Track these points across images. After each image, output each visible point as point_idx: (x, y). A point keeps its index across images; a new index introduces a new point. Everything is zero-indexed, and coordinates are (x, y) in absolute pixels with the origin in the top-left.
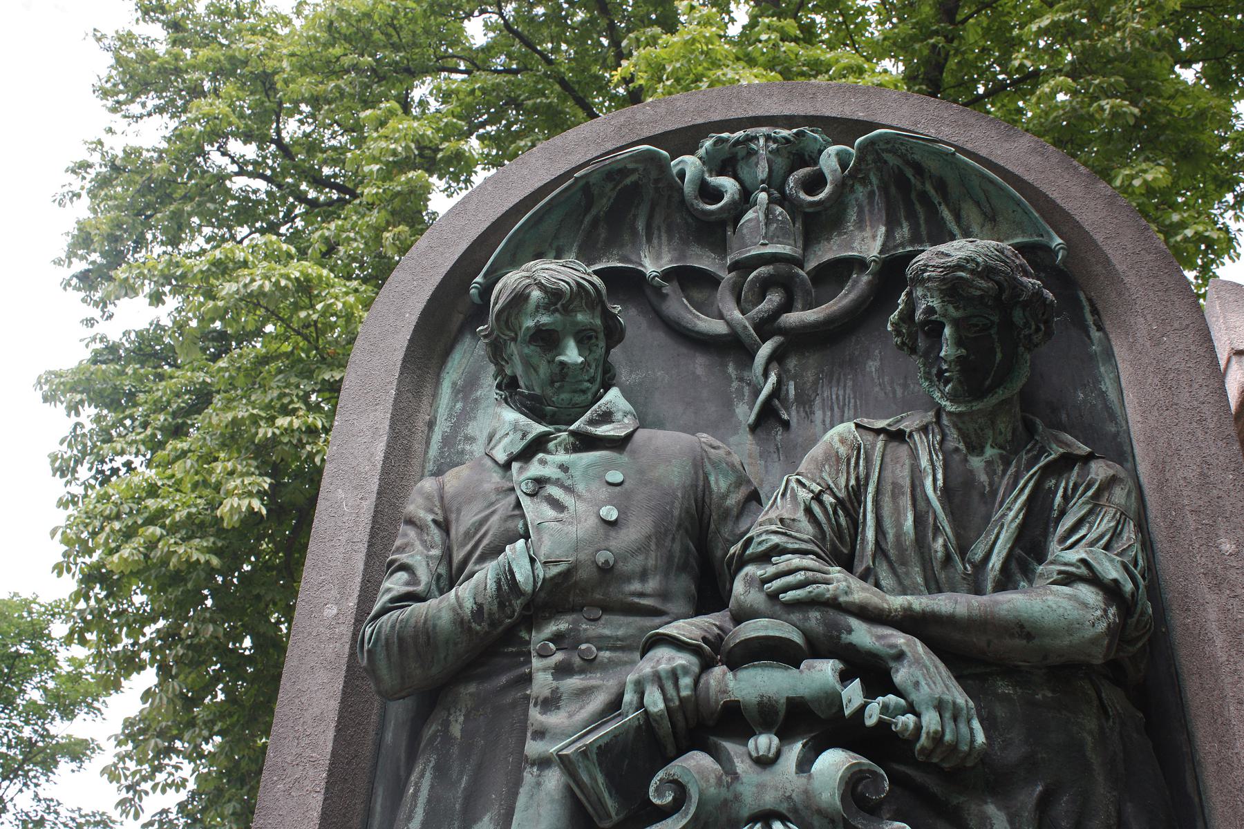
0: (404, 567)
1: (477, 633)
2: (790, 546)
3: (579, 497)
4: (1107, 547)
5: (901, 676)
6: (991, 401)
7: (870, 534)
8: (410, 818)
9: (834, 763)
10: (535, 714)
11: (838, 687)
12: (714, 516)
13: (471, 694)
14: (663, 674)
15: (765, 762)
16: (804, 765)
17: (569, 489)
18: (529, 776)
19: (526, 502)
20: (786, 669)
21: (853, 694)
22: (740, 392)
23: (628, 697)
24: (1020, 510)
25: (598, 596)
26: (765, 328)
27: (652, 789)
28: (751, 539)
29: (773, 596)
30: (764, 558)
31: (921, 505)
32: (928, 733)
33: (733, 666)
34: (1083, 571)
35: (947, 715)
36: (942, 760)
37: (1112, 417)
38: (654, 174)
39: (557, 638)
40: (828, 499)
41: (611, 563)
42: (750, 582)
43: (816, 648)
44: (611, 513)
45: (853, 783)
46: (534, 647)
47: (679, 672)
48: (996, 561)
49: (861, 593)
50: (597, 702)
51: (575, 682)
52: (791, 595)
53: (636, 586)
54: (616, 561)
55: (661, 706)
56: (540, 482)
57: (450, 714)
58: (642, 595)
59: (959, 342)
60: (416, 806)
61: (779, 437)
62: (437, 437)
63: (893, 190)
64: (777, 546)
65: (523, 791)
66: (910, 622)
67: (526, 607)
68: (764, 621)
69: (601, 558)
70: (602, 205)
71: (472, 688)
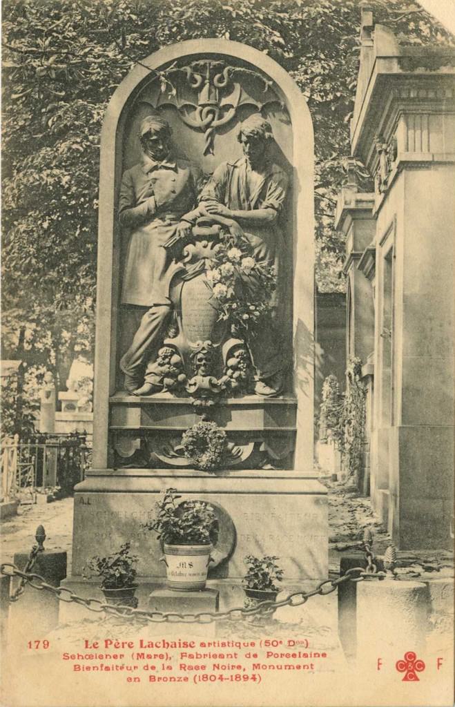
34: (270, 206)
40: (220, 185)
43: (215, 222)
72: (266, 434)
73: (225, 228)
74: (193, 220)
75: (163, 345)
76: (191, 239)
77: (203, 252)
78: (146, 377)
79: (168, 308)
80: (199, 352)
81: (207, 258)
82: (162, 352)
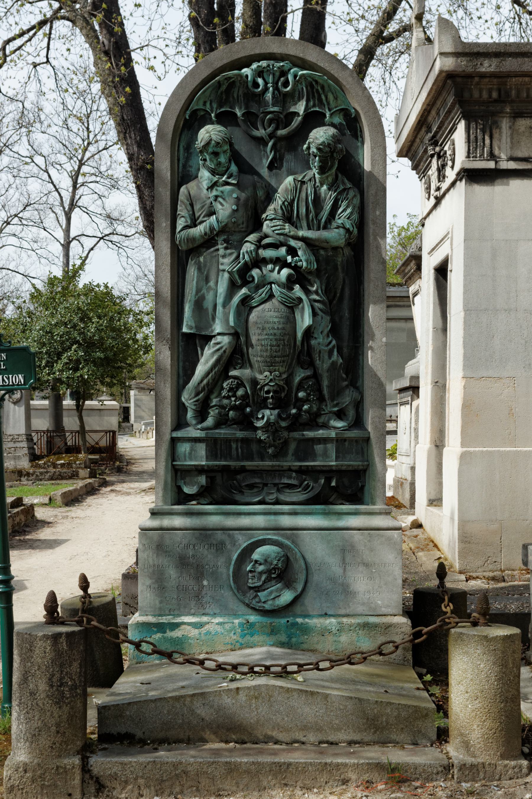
3: (227, 202)
4: (348, 218)
6: (327, 174)
9: (285, 272)
10: (221, 260)
16: (279, 272)
17: (224, 199)
18: (221, 273)
19: (214, 203)
22: (264, 155)
23: (241, 256)
26: (271, 136)
38: (239, 79)
40: (286, 203)
42: (268, 226)
43: (282, 244)
44: (235, 207)
45: (289, 277)
46: (219, 242)
51: (229, 251)
52: (277, 232)
56: (216, 197)
59: (320, 161)
62: (181, 165)
63: (309, 88)
65: (220, 277)
69: (233, 220)
70: (224, 87)
72: (339, 472)
73: (292, 251)
74: (258, 241)
75: (228, 377)
76: (258, 262)
77: (270, 277)
78: (210, 411)
79: (231, 337)
80: (267, 384)
81: (274, 283)
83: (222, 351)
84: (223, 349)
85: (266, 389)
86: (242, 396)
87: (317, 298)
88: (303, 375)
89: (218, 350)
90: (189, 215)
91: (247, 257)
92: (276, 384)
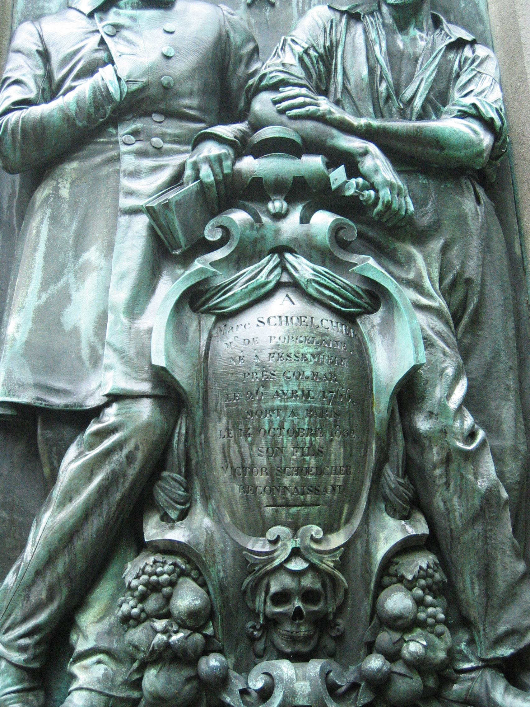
0: (17, 82)
1: (79, 127)
2: (291, 81)
5: (367, 164)
7: (340, 78)
8: (35, 250)
11: (326, 171)
12: (232, 60)
13: (74, 169)
14: (213, 160)
15: (279, 216)
16: (305, 219)
19: (107, 39)
20: (293, 159)
21: (338, 175)
23: (188, 172)
24: (434, 70)
25: (163, 106)
27: (206, 232)
28: (264, 76)
29: (282, 112)
30: (275, 87)
31: (372, 61)
32: (383, 202)
33: (256, 156)
34: (473, 111)
35: (395, 192)
36: (388, 220)
37: (481, 20)
39: (135, 133)
41: (172, 85)
47: (223, 157)
48: (418, 103)
49: (338, 113)
50: (165, 176)
53: (186, 102)
54: (174, 84)
55: (212, 178)
57: (58, 183)
58: (190, 108)
60: (39, 242)
61: (267, 14)
64: (283, 80)
66: (367, 134)
67: (114, 111)
68: (277, 128)
71: (75, 165)
77: (277, 232)
78: (75, 669)
81: (292, 251)
82: (136, 570)
83: (119, 457)
84: (125, 451)
85: (274, 588)
86: (193, 614)
87: (424, 301)
88: (399, 537)
89: (108, 453)
90: (35, 76)
91: (206, 173)
92: (313, 567)
